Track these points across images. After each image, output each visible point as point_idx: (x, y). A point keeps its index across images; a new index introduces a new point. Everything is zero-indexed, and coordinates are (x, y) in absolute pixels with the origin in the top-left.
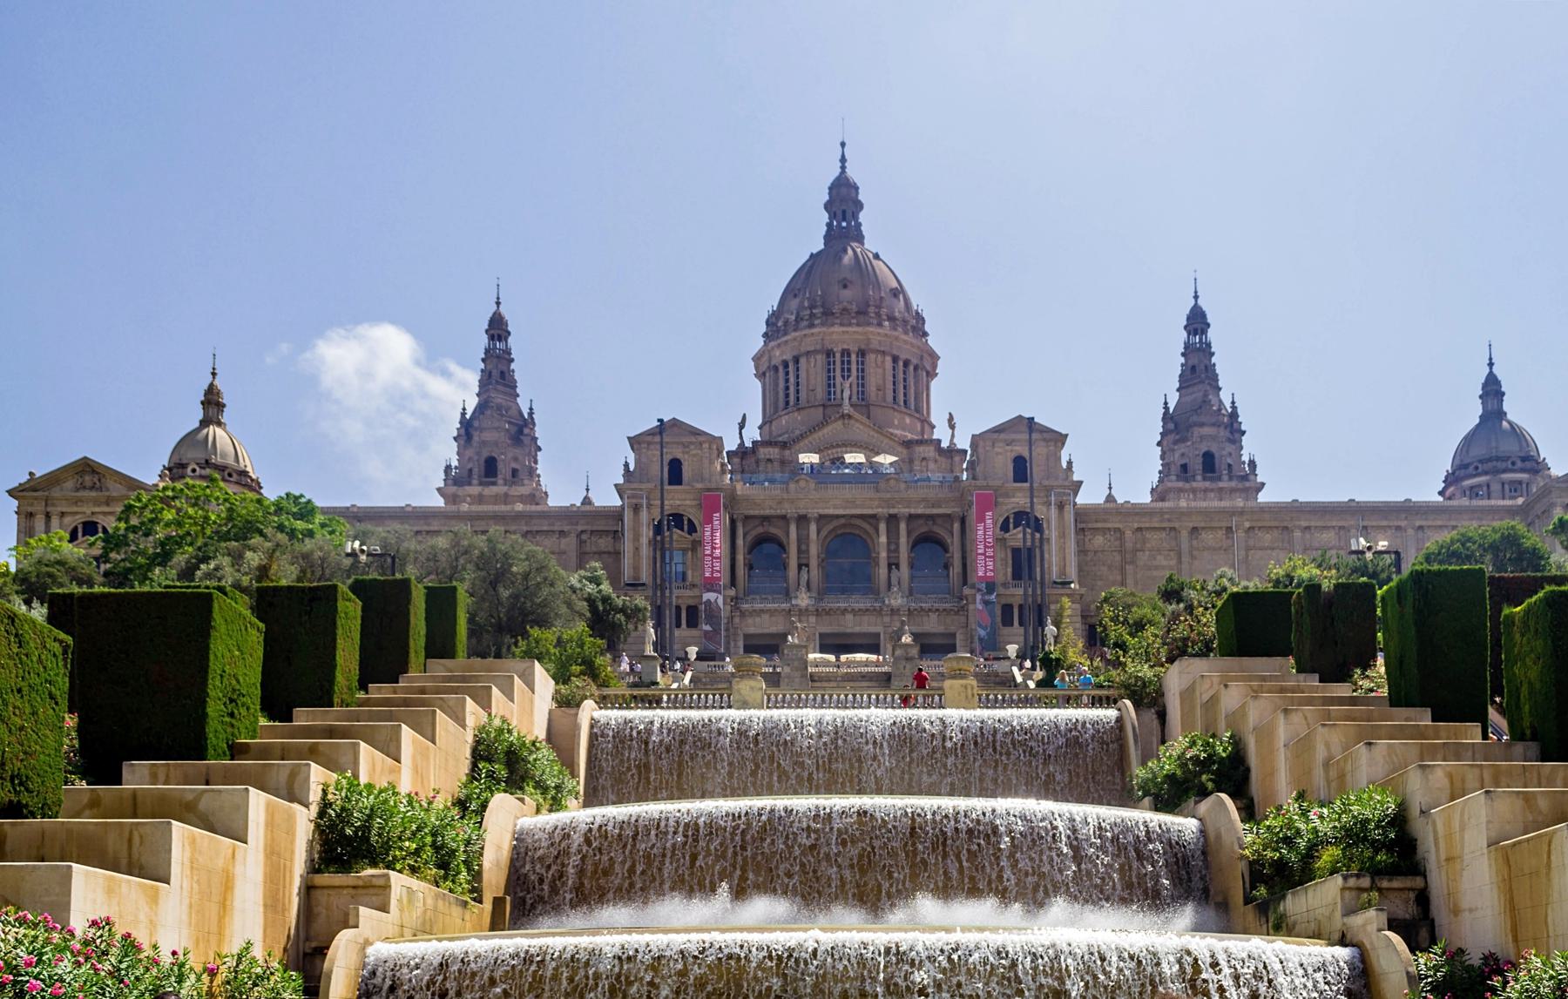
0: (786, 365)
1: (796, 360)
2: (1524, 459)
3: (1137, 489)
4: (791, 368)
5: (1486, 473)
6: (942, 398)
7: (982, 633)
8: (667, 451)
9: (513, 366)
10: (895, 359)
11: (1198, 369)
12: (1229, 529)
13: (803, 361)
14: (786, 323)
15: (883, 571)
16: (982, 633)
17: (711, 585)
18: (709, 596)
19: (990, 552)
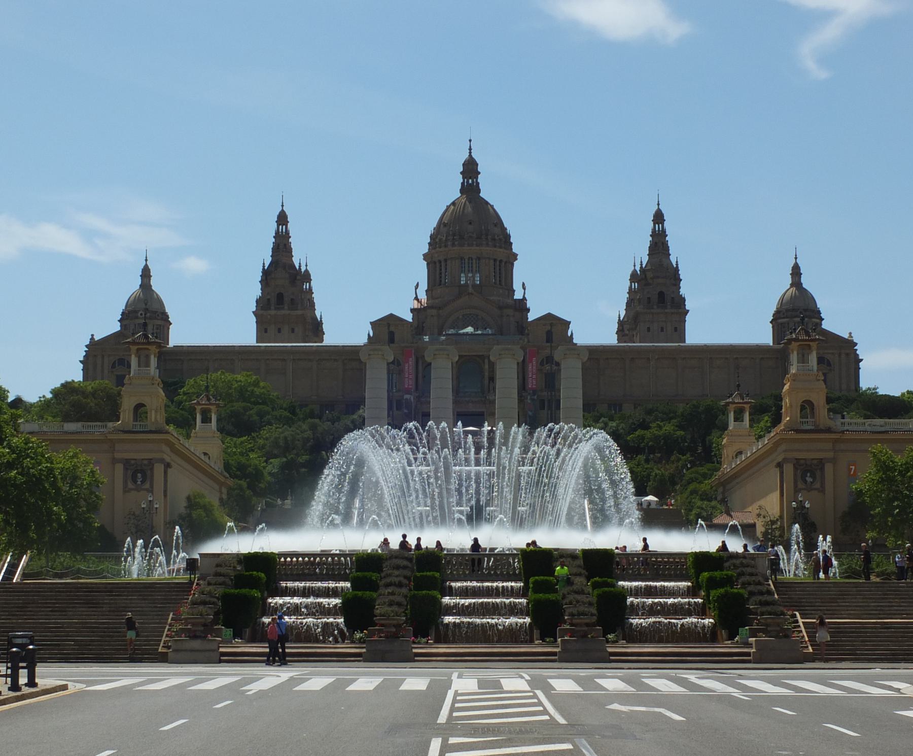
0: (440, 262)
1: (446, 260)
2: (806, 310)
3: (608, 337)
4: (443, 264)
5: (787, 317)
6: (520, 274)
7: (530, 413)
8: (386, 327)
9: (290, 240)
10: (495, 260)
11: (659, 244)
12: (648, 359)
13: (449, 262)
14: (440, 240)
15: (486, 381)
16: (530, 413)
17: (408, 392)
18: (407, 396)
19: (534, 376)
